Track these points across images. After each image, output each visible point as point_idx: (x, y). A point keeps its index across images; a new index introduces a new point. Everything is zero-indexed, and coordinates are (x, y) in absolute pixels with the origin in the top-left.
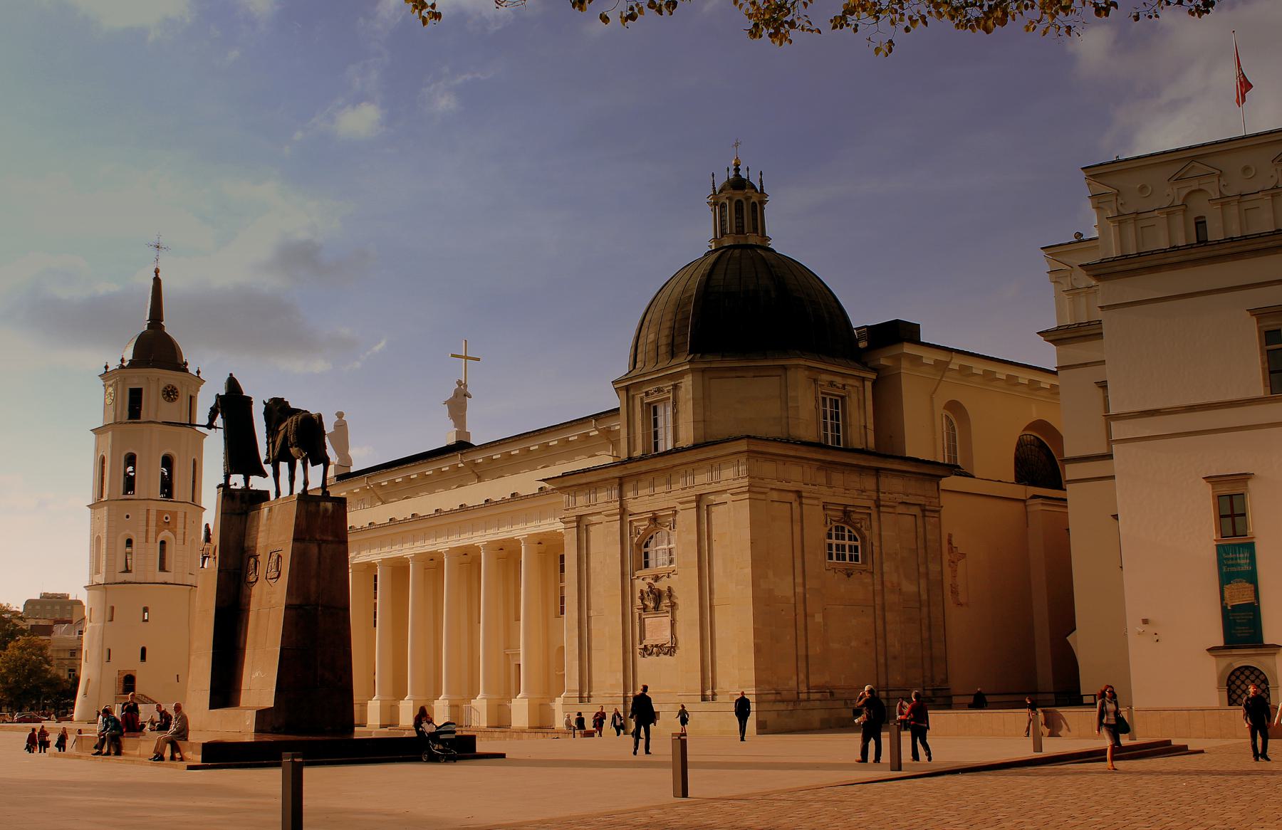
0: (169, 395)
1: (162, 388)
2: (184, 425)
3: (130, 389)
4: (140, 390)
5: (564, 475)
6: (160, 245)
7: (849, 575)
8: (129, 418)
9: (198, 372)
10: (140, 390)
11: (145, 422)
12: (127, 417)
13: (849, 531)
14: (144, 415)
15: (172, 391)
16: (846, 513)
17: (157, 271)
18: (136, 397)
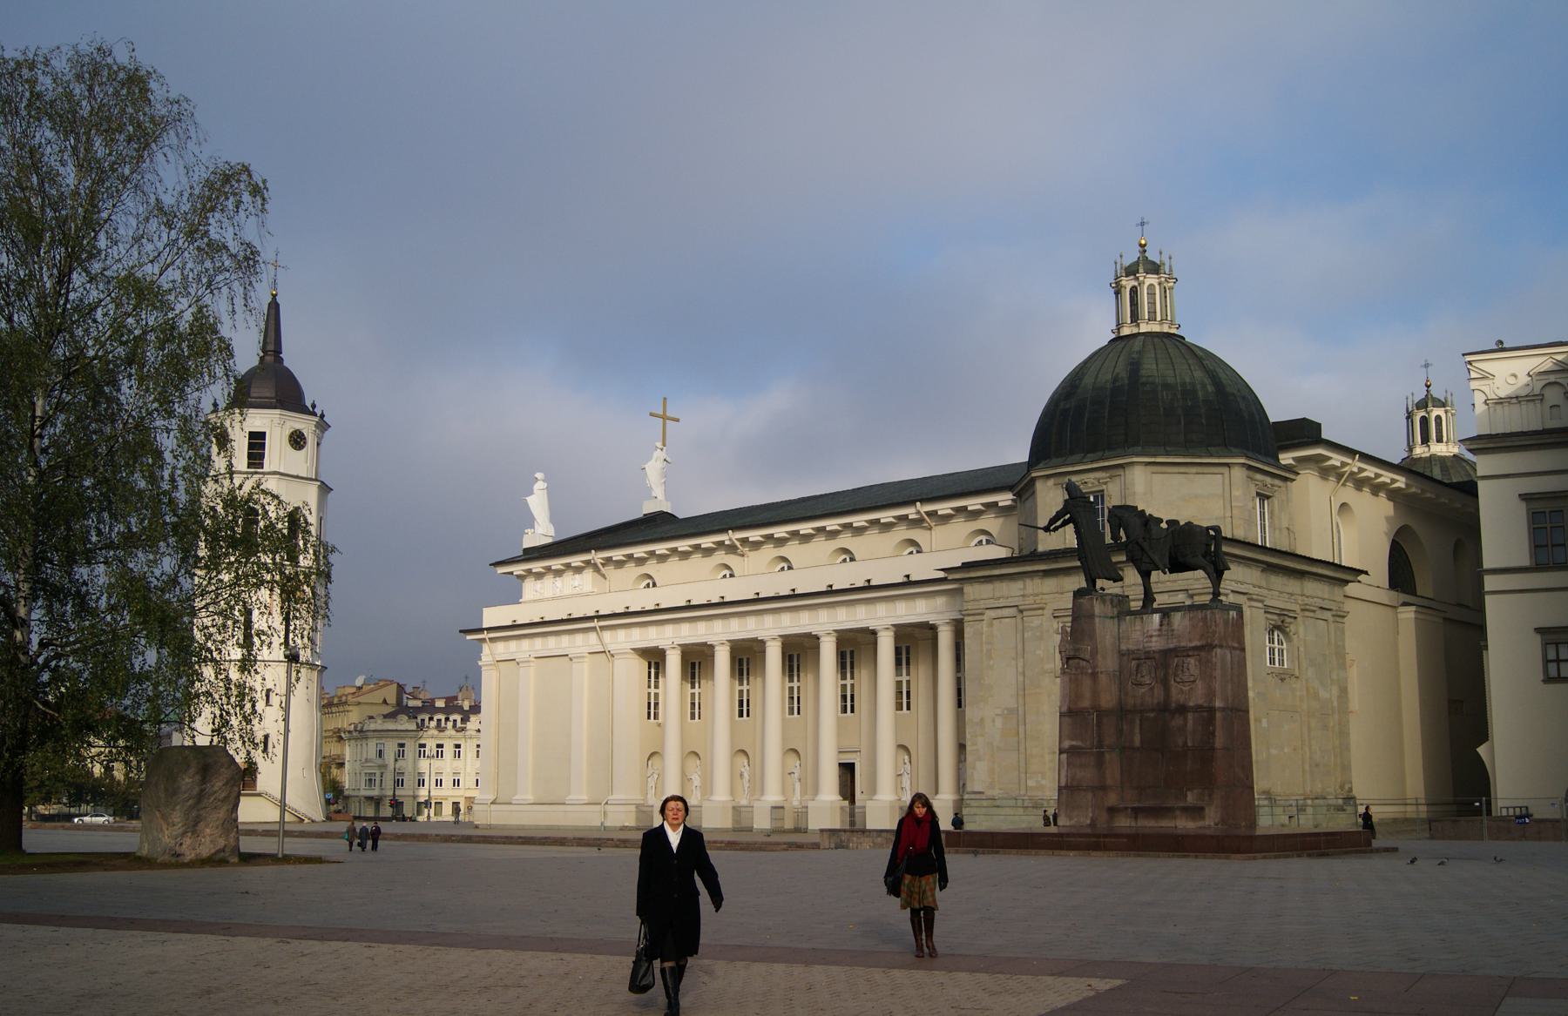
0: (295, 441)
1: (288, 432)
2: (311, 479)
3: (252, 435)
4: (262, 435)
5: (967, 566)
6: (279, 263)
7: (1282, 680)
8: (248, 467)
9: (322, 416)
10: (262, 435)
11: (269, 473)
12: (246, 465)
13: (1278, 636)
14: (269, 463)
15: (298, 437)
16: (1283, 614)
17: (274, 296)
18: (257, 441)
